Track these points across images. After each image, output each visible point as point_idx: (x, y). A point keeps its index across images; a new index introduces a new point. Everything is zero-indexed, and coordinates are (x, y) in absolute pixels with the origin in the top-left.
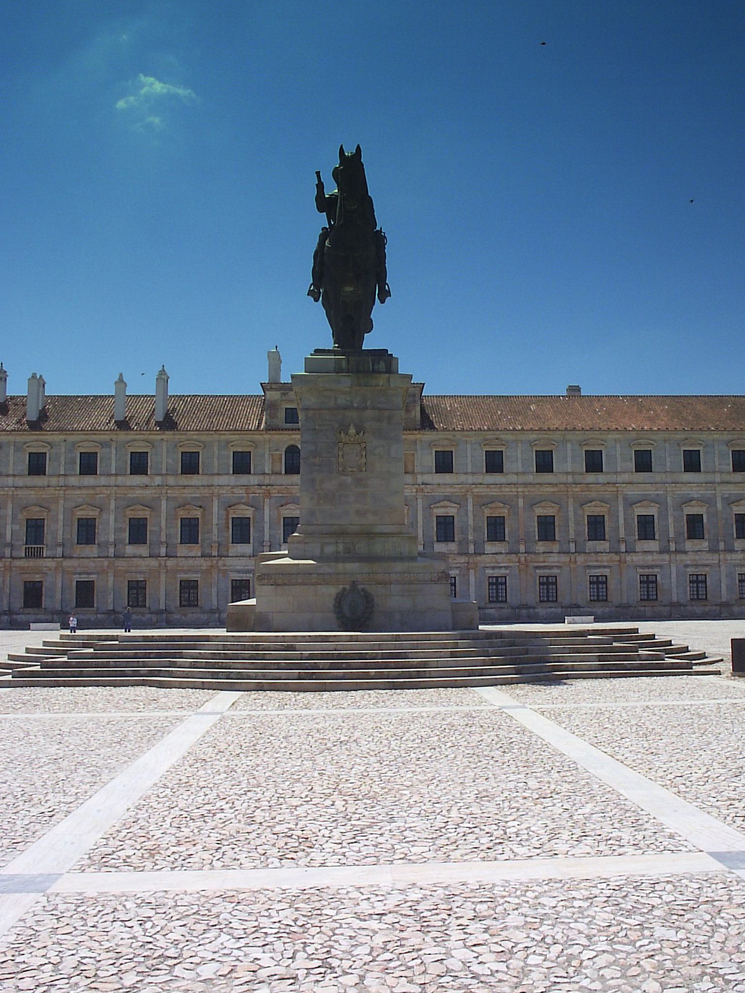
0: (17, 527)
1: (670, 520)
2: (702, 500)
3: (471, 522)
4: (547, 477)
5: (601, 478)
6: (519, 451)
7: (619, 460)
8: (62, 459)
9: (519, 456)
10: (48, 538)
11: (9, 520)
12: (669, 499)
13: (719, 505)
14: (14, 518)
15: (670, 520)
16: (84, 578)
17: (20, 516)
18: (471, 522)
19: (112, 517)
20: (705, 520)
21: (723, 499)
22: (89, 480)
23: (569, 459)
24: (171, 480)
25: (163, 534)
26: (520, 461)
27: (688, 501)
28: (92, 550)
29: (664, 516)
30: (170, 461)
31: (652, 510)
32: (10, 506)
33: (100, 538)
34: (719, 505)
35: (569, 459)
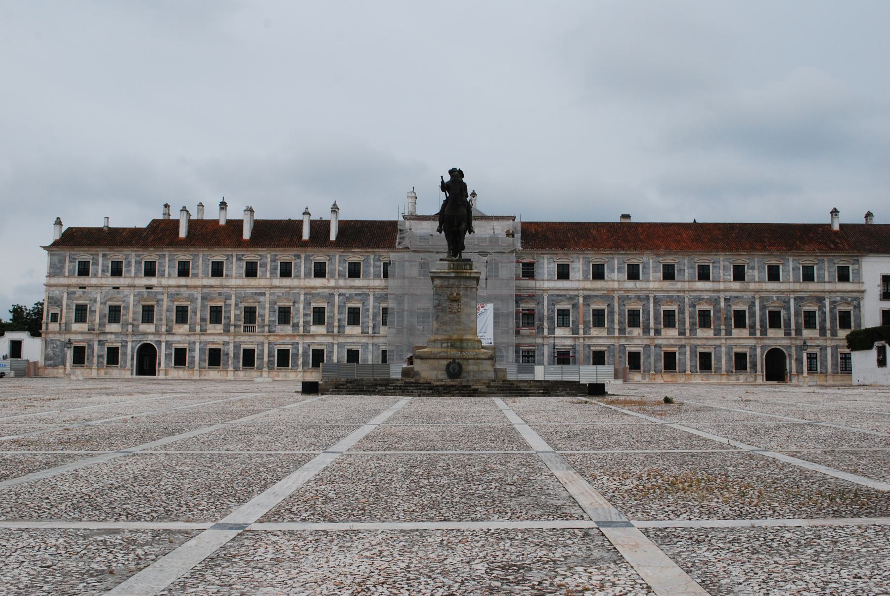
0: (238, 312)
1: (687, 314)
2: (710, 301)
3: (546, 313)
4: (599, 284)
5: (639, 285)
7: (651, 271)
8: (268, 267)
10: (259, 320)
11: (233, 307)
12: (686, 300)
13: (722, 304)
14: (236, 305)
15: (687, 314)
16: (282, 347)
17: (240, 305)
18: (546, 313)
19: (302, 306)
20: (712, 314)
21: (725, 299)
22: (286, 282)
23: (616, 271)
24: (342, 282)
25: (336, 318)
26: (581, 272)
27: (700, 299)
28: (288, 329)
29: (682, 312)
31: (674, 307)
32: (233, 297)
33: (293, 320)
34: (722, 304)
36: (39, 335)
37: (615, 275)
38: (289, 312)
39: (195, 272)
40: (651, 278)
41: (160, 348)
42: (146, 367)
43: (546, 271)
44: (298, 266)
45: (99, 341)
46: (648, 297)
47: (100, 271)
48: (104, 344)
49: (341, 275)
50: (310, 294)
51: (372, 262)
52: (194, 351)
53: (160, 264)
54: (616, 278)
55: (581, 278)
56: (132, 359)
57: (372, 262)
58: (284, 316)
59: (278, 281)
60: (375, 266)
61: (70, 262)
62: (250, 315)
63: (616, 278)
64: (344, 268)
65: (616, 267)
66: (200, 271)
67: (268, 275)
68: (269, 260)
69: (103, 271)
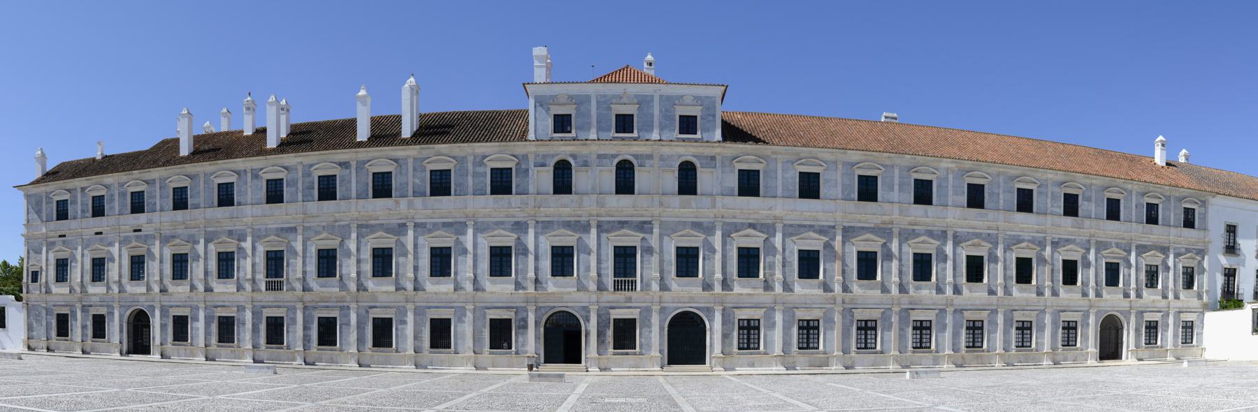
6: (839, 173)
7: (950, 193)
9: (839, 180)
23: (896, 187)
26: (840, 188)
30: (417, 181)
35: (896, 187)
37: (895, 195)
38: (335, 257)
40: (950, 203)
41: (154, 316)
43: (780, 182)
46: (945, 232)
49: (418, 193)
50: (367, 226)
51: (470, 167)
52: (197, 320)
54: (896, 200)
55: (840, 196)
56: (121, 331)
57: (470, 167)
58: (327, 263)
60: (475, 175)
62: (275, 263)
63: (896, 200)
64: (423, 180)
65: (896, 181)
66: (202, 199)
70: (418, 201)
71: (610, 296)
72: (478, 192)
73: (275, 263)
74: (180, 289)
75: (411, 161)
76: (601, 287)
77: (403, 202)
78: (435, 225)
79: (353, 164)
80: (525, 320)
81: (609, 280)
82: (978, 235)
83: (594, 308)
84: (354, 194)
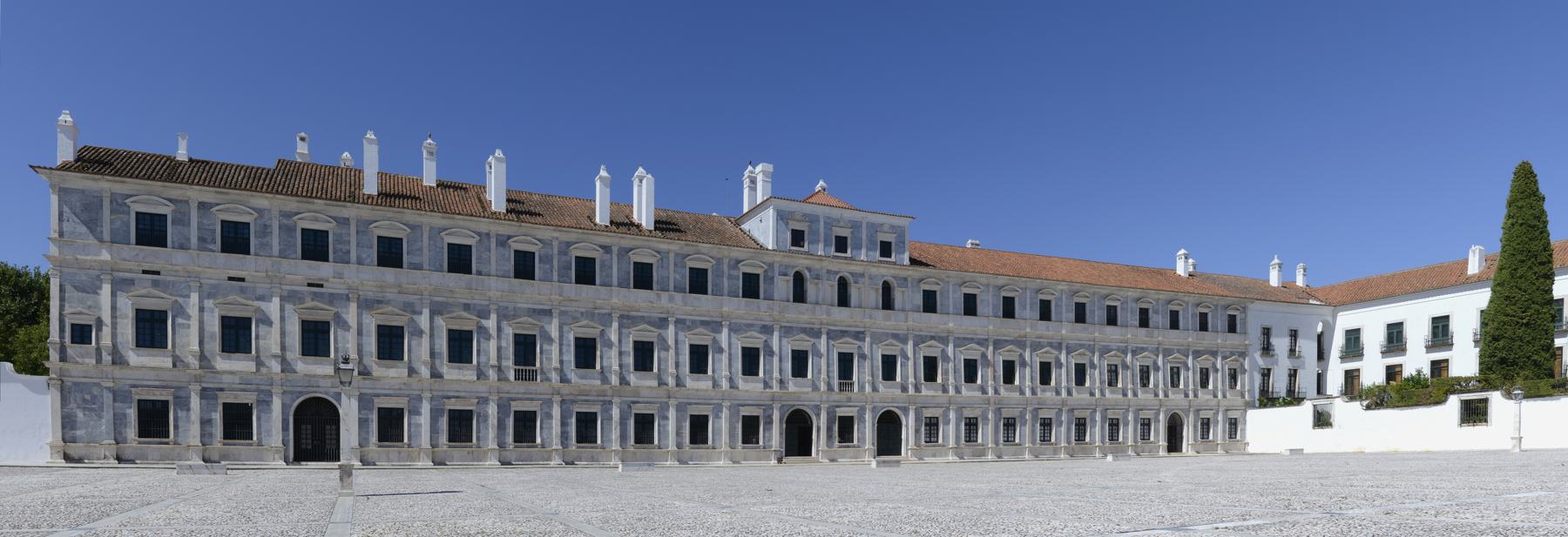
36: (46, 372)
39: (416, 260)
42: (307, 444)
44: (607, 267)
45: (204, 389)
47: (194, 240)
48: (216, 398)
50: (628, 317)
53: (339, 240)
59: (573, 289)
61: (112, 212)
64: (683, 277)
67: (555, 277)
68: (556, 251)
69: (201, 239)
70: (678, 296)
71: (837, 396)
72: (732, 294)
73: (525, 349)
74: (392, 372)
75: (672, 255)
76: (830, 388)
77: (664, 295)
78: (693, 322)
79: (615, 249)
80: (770, 417)
81: (836, 382)
82: (1082, 346)
83: (824, 407)
84: (615, 282)
